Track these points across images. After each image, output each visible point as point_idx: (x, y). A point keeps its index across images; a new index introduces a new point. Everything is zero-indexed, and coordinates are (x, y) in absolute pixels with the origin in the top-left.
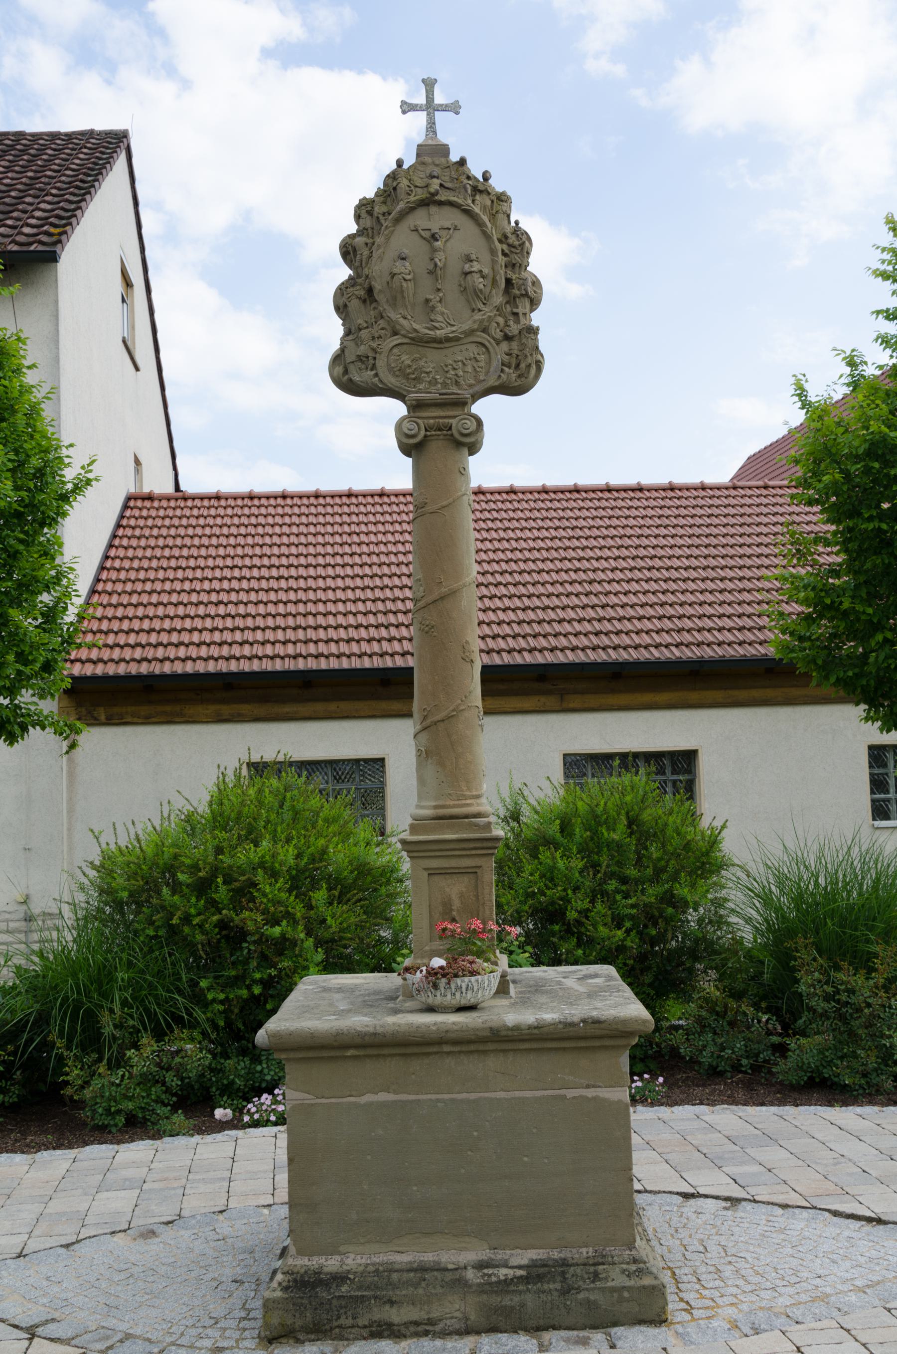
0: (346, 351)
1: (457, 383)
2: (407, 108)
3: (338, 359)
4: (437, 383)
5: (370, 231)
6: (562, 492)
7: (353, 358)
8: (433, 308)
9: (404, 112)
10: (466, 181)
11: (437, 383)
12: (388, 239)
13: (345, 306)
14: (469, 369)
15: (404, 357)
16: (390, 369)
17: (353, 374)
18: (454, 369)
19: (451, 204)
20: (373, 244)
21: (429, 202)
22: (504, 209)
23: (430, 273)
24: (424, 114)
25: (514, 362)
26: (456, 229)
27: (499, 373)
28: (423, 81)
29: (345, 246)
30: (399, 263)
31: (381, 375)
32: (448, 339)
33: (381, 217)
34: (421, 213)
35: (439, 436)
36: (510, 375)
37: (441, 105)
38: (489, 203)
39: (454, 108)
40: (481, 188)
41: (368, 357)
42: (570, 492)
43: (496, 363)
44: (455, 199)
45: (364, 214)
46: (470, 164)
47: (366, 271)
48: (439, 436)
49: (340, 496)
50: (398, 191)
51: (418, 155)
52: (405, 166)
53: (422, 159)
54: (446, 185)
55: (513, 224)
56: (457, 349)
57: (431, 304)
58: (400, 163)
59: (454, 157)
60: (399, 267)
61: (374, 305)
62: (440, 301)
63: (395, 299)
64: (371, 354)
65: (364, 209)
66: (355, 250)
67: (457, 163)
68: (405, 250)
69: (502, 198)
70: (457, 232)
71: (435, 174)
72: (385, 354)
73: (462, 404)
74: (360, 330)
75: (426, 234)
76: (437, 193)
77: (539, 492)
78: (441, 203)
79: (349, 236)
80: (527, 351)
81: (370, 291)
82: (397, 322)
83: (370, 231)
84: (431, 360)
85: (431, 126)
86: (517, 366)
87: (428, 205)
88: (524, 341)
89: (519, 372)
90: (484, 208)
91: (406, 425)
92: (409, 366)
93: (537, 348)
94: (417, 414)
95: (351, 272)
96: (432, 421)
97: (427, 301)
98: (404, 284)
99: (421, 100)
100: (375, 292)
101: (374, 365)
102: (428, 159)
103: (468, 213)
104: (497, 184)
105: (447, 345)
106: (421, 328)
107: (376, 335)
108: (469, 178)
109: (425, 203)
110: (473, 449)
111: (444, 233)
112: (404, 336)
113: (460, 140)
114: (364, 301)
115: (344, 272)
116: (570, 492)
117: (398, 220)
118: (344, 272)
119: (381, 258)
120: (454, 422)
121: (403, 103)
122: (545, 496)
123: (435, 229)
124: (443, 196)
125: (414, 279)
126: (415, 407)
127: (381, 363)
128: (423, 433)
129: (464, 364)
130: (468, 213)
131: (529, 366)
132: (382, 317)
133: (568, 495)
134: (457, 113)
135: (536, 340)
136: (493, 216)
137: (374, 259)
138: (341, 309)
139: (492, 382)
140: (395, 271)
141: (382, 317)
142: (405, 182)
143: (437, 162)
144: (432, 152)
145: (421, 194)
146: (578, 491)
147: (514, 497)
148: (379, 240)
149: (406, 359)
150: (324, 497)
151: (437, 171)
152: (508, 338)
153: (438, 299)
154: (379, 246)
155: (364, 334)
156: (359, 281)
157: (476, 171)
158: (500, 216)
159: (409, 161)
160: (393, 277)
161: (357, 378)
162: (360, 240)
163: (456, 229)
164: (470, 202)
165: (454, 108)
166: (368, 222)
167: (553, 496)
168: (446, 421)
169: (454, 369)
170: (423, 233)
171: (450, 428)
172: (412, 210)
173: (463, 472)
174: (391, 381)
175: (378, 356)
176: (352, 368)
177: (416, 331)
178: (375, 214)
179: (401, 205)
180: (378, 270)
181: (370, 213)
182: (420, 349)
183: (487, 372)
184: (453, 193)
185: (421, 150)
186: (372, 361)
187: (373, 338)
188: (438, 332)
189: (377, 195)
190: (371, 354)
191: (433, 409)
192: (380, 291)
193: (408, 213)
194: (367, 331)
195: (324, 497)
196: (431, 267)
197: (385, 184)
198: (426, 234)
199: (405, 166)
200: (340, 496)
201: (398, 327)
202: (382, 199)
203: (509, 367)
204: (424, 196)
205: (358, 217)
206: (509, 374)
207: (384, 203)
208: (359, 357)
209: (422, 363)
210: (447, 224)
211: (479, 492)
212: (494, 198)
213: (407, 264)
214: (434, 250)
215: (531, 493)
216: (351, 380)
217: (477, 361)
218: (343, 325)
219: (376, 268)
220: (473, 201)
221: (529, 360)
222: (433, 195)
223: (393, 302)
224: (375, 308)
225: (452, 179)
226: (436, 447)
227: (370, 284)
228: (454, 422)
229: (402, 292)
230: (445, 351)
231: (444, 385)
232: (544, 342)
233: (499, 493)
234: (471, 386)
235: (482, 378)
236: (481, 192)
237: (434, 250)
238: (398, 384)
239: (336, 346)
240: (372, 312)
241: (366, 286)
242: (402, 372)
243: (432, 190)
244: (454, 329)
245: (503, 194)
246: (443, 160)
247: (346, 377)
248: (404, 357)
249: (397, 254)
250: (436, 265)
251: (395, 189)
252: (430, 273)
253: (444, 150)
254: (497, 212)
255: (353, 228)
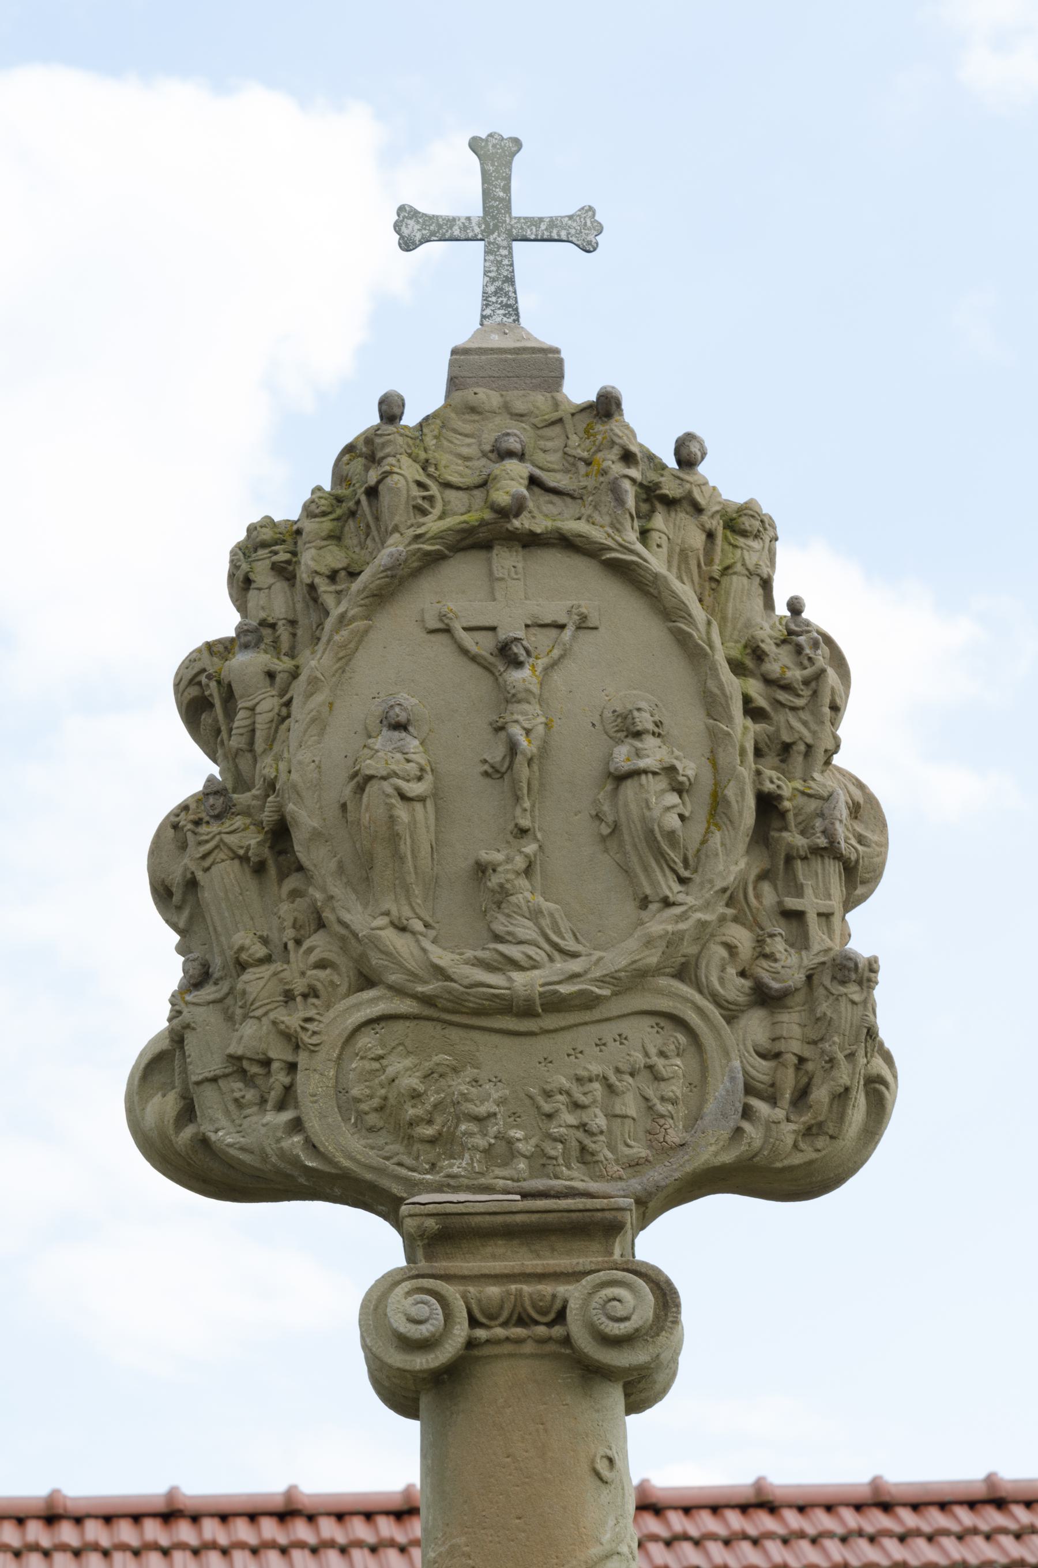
0: (190, 1038)
1: (585, 1156)
2: (415, 229)
3: (159, 1067)
4: (512, 1154)
5: (284, 633)
6: (943, 1506)
7: (215, 1065)
8: (502, 896)
9: (407, 245)
10: (618, 469)
11: (512, 1154)
12: (345, 659)
13: (192, 884)
14: (630, 1105)
15: (396, 1065)
16: (349, 1107)
17: (214, 1124)
18: (577, 1106)
19: (567, 543)
20: (295, 675)
21: (493, 535)
22: (751, 559)
23: (494, 773)
24: (472, 255)
25: (788, 1081)
26: (583, 625)
27: (735, 1119)
28: (475, 145)
29: (194, 681)
30: (383, 740)
31: (313, 1124)
32: (555, 1004)
33: (323, 586)
34: (463, 573)
35: (518, 1337)
36: (776, 1128)
37: (537, 222)
38: (697, 540)
39: (581, 232)
40: (669, 490)
41: (267, 1063)
42: (972, 1505)
43: (723, 1088)
44: (581, 527)
45: (263, 576)
46: (632, 413)
47: (266, 767)
48: (518, 1337)
49: (137, 1518)
50: (385, 498)
51: (454, 383)
52: (411, 418)
53: (467, 395)
54: (551, 480)
55: (781, 609)
56: (584, 1038)
57: (494, 881)
58: (390, 409)
59: (579, 389)
60: (385, 754)
61: (293, 882)
62: (528, 871)
63: (367, 862)
64: (278, 1052)
65: (264, 559)
66: (229, 696)
67: (588, 408)
68: (410, 701)
69: (745, 525)
70: (585, 636)
71: (513, 444)
72: (330, 1051)
73: (604, 1228)
74: (242, 967)
75: (482, 645)
76: (518, 507)
77: (858, 1507)
78: (531, 541)
79: (209, 647)
80: (835, 1046)
81: (280, 833)
82: (374, 943)
83: (284, 633)
84: (493, 1074)
85: (501, 293)
86: (802, 1096)
87: (486, 546)
88: (824, 1007)
89: (807, 1115)
90: (681, 556)
91: (402, 1306)
92: (416, 1096)
93: (871, 1033)
94: (443, 1265)
95: (215, 770)
96: (494, 1291)
97: (482, 870)
98: (402, 812)
99: (459, 193)
100: (299, 837)
101: (289, 1089)
102: (488, 397)
103: (625, 572)
104: (727, 478)
105: (550, 1021)
106: (461, 965)
107: (299, 986)
108: (628, 457)
109: (473, 542)
110: (642, 1389)
111: (540, 640)
112: (398, 991)
113: (594, 330)
114: (259, 869)
115: (187, 769)
116: (972, 1505)
117: (381, 597)
118: (187, 769)
119: (319, 723)
120: (573, 1293)
121: (406, 214)
122: (880, 1520)
123: (511, 628)
124: (541, 517)
125: (436, 794)
126: (435, 1240)
127: (314, 1083)
128: (461, 1331)
129: (610, 1088)
130: (625, 572)
131: (843, 1096)
132: (321, 925)
133: (965, 1517)
134: (589, 248)
135: (868, 1005)
136: (712, 585)
137: (297, 725)
138: (176, 894)
139: (711, 1151)
140: (371, 766)
141: (321, 925)
142: (408, 471)
143: (520, 406)
144: (501, 373)
145: (461, 512)
146: (1000, 1503)
147: (766, 1522)
148: (315, 662)
149: (404, 1071)
150: (78, 1520)
151: (518, 436)
152: (765, 998)
153: (520, 863)
154: (314, 683)
155: (256, 982)
156: (242, 799)
157: (652, 430)
158: (737, 583)
159: (424, 398)
160: (361, 789)
161: (225, 1136)
162: (248, 663)
163: (583, 625)
164: (632, 536)
165: (581, 232)
166: (276, 601)
167: (909, 1519)
168: (546, 1289)
169: (577, 1106)
170: (468, 640)
171: (561, 1317)
172: (431, 561)
173: (605, 1469)
174: (351, 1147)
175: (302, 1059)
176: (208, 1099)
177: (440, 972)
178: (303, 576)
179: (395, 548)
180: (311, 763)
181: (285, 572)
182: (454, 1034)
183: (694, 1119)
184: (571, 508)
185: (465, 368)
186: (281, 1078)
187: (289, 997)
188: (519, 978)
189: (310, 511)
190: (278, 1052)
191: (499, 1247)
192: (316, 835)
193: (416, 573)
194: (265, 971)
195: (78, 1520)
196: (497, 754)
197: (340, 476)
198: (482, 645)
199: (411, 418)
200: (137, 1518)
201: (376, 960)
202: (326, 525)
203: (773, 1100)
204: (473, 518)
205: (241, 585)
206: (771, 1124)
207: (336, 537)
208: (236, 1066)
209: (460, 1085)
210: (553, 610)
211: (650, 1506)
212: (717, 524)
213: (413, 744)
214: (509, 698)
215: (829, 1508)
216: (204, 1142)
217: (658, 1078)
218: (181, 949)
219: (304, 756)
220: (644, 534)
221: (843, 1075)
222: (504, 513)
223: (363, 873)
224: (295, 894)
225: (570, 462)
226: (509, 1384)
227: (280, 810)
228: (573, 1293)
229: (394, 838)
230: (544, 1044)
231: (541, 1162)
232: (896, 1014)
233: (715, 1509)
234: (635, 1165)
235: (674, 1137)
236: (670, 503)
237: (509, 698)
238: (374, 1158)
239: (156, 1020)
240: (284, 908)
241: (267, 816)
242: (389, 1117)
243: (501, 497)
244: (575, 966)
245: (748, 510)
246: (540, 400)
247: (189, 1131)
248: (396, 1065)
249: (376, 709)
250: (513, 748)
251: (372, 492)
252: (494, 773)
253: (544, 367)
254: (726, 570)
255: (225, 621)
